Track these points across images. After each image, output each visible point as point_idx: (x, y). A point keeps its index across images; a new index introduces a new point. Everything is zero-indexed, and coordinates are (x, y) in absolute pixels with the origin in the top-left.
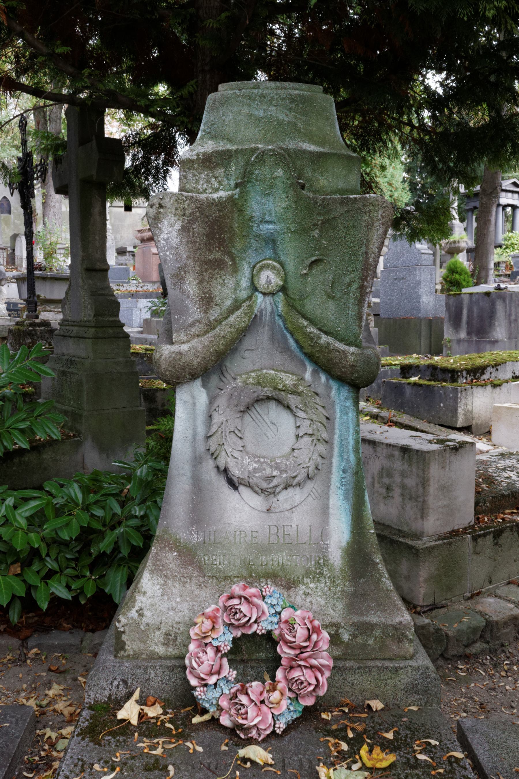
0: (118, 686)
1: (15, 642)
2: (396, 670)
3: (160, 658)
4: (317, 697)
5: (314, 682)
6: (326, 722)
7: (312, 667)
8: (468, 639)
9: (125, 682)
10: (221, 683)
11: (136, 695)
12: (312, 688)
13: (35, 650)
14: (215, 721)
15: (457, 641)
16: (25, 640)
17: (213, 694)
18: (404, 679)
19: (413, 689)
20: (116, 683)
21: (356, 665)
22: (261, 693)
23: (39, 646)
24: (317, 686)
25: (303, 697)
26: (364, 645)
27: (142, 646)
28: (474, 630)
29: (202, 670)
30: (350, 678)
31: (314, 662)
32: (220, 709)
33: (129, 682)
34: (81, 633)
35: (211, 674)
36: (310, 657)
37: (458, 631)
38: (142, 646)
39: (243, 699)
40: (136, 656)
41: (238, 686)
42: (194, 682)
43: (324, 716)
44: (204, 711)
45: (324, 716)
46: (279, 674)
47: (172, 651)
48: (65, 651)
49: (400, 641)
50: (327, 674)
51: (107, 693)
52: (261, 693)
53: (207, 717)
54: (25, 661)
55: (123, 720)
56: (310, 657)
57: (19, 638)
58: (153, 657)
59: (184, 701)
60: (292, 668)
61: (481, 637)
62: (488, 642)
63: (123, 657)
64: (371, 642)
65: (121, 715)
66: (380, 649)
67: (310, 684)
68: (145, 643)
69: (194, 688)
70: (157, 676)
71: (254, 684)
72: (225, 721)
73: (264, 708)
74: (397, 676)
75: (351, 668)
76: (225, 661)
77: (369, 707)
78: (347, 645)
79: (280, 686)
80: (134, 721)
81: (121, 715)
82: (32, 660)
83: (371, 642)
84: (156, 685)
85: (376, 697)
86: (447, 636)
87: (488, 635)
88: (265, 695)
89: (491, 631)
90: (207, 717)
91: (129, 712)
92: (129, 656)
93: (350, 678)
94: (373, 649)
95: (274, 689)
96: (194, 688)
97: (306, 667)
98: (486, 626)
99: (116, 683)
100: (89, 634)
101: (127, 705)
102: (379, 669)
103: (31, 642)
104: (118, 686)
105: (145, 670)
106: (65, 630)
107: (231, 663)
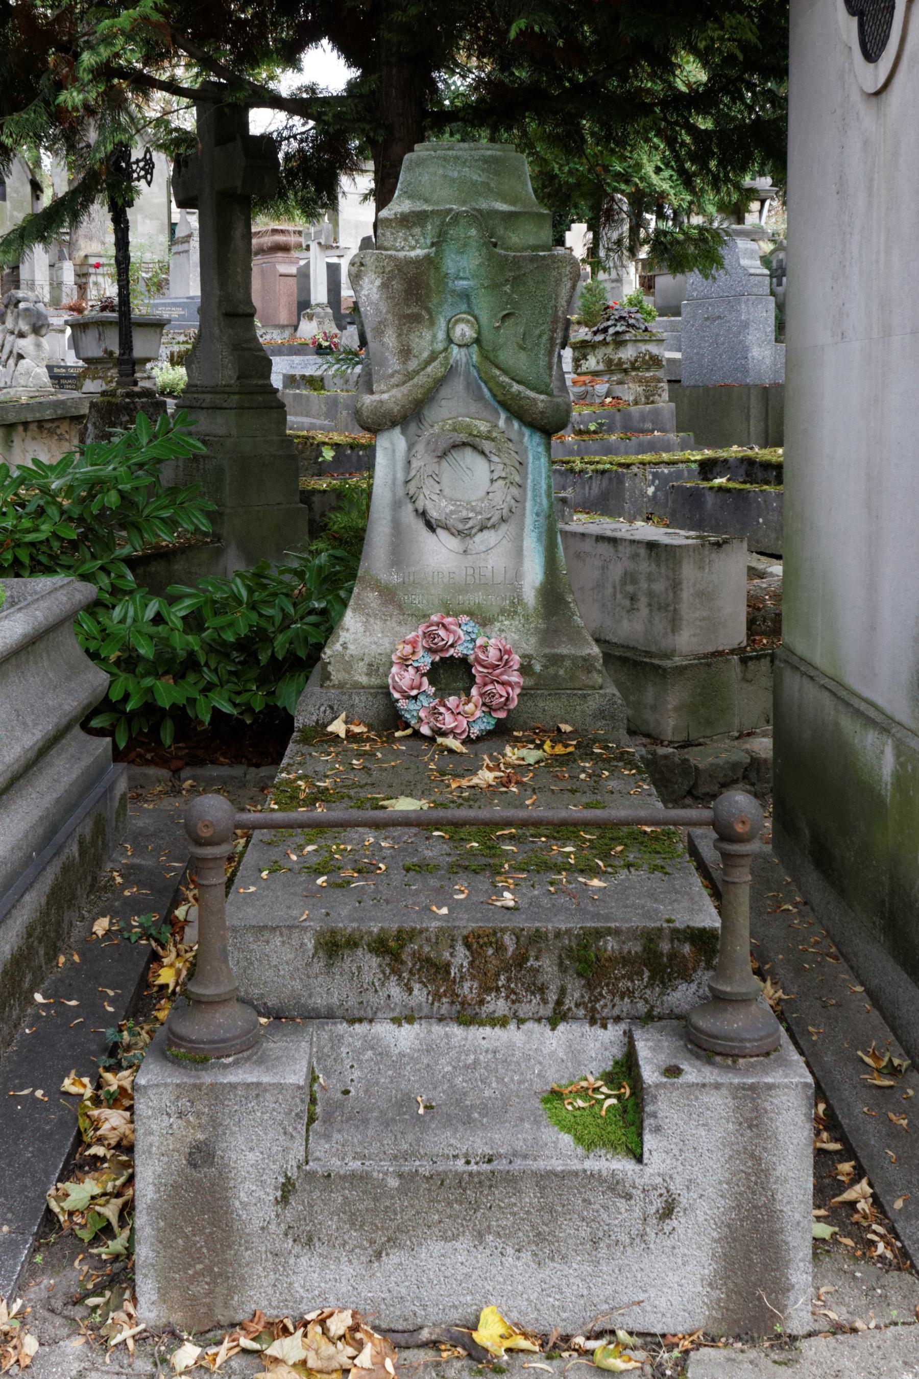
0: (325, 712)
1: (164, 773)
2: (585, 696)
3: (364, 687)
4: (509, 711)
5: (504, 694)
6: (517, 737)
7: (503, 684)
8: (725, 776)
9: (331, 707)
10: (421, 697)
11: (343, 716)
12: (503, 699)
13: (190, 782)
14: (417, 734)
15: (710, 776)
16: (176, 772)
17: (412, 706)
18: (593, 704)
19: (600, 714)
20: (323, 708)
21: (546, 693)
22: (458, 706)
23: (194, 778)
24: (507, 699)
25: (495, 710)
26: (556, 676)
27: (347, 676)
28: (735, 766)
29: (404, 684)
30: (541, 704)
31: (505, 678)
32: (420, 720)
33: (335, 707)
34: (244, 767)
35: (412, 688)
36: (502, 674)
37: (712, 764)
38: (347, 676)
39: (442, 710)
40: (341, 686)
41: (437, 701)
42: (396, 695)
43: (515, 733)
44: (407, 725)
45: (515, 733)
46: (474, 691)
47: (375, 681)
48: (225, 783)
49: (589, 672)
50: (518, 691)
51: (314, 718)
52: (458, 706)
53: (409, 731)
54: (180, 792)
55: (332, 733)
56: (502, 674)
57: (169, 769)
58: (357, 686)
60: (485, 685)
61: (745, 777)
62: (753, 784)
63: (328, 687)
64: (561, 672)
65: (330, 729)
66: (571, 678)
67: (501, 696)
68: (349, 673)
69: (397, 701)
70: (360, 701)
71: (451, 698)
72: (425, 730)
73: (460, 717)
74: (586, 702)
75: (542, 695)
76: (425, 680)
77: (559, 730)
78: (540, 676)
79: (474, 700)
80: (343, 735)
81: (330, 729)
82: (188, 791)
83: (561, 672)
84: (360, 711)
85: (566, 722)
86: (697, 768)
87: (753, 776)
88: (461, 707)
89: (758, 771)
90: (409, 731)
91: (338, 727)
92: (334, 686)
93: (541, 704)
94: (564, 679)
95: (469, 701)
96: (397, 701)
97: (498, 682)
98: (751, 764)
99: (323, 708)
100: (252, 769)
101: (335, 722)
102: (569, 696)
103: (184, 774)
104: (325, 712)
105: (350, 696)
106: (222, 764)
107: (431, 683)
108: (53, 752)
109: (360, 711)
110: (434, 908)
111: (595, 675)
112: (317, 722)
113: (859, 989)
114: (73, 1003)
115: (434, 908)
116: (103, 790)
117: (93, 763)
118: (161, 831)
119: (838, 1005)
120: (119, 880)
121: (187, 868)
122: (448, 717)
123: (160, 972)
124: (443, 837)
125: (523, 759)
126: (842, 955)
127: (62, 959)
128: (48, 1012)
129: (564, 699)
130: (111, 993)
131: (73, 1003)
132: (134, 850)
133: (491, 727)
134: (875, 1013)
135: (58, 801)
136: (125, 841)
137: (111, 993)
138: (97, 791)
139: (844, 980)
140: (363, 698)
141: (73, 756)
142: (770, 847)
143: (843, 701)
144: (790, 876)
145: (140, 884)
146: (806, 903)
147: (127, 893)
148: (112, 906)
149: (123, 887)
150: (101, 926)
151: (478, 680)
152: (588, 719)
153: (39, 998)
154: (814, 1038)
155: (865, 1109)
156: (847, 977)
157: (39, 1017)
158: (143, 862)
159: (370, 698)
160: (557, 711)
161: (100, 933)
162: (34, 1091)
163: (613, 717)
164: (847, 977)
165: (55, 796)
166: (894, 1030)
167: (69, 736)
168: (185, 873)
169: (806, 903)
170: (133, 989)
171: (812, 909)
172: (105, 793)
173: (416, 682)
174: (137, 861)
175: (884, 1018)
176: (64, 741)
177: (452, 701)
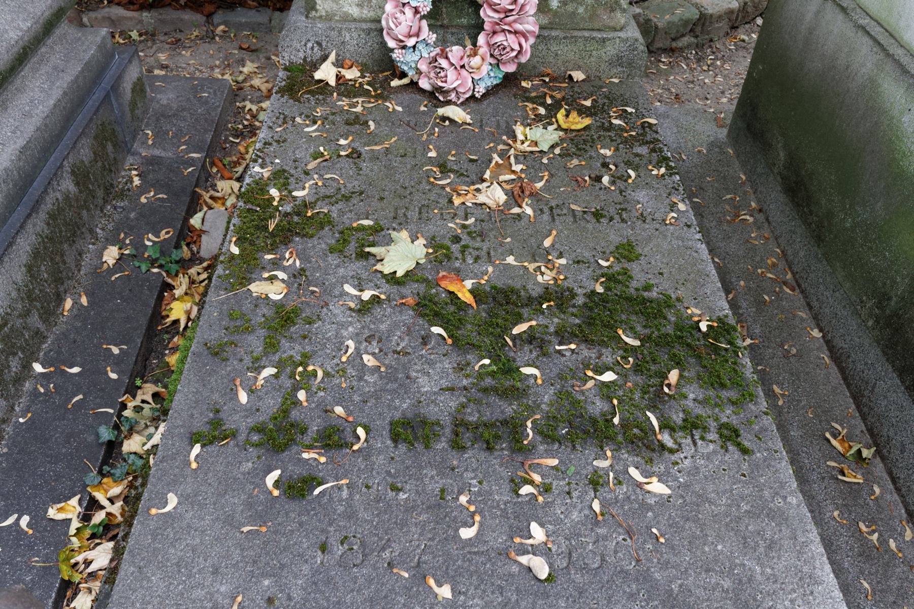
0: (312, 48)
1: (199, 18)
2: (604, 40)
3: (355, 20)
4: (519, 64)
5: (517, 47)
6: (526, 90)
7: (516, 33)
8: (678, 32)
9: (319, 44)
10: (420, 46)
11: (332, 57)
12: (514, 54)
13: (222, 27)
14: (414, 84)
15: (666, 33)
16: (209, 16)
17: (411, 57)
18: (611, 50)
19: (618, 61)
20: (310, 45)
21: (562, 35)
22: (462, 58)
23: (225, 23)
24: (520, 52)
25: (504, 63)
26: (574, 13)
27: (335, 7)
28: (686, 22)
29: (400, 31)
30: (554, 48)
31: (518, 27)
32: (419, 72)
33: (324, 44)
34: (269, 11)
35: (409, 36)
36: (515, 21)
37: (669, 23)
38: (335, 7)
39: (444, 63)
40: (329, 18)
41: (438, 50)
42: (391, 44)
43: (524, 84)
44: (403, 75)
45: (524, 84)
46: (481, 39)
47: (367, 13)
48: (254, 30)
49: (613, 10)
50: (532, 40)
51: (301, 55)
52: (462, 58)
53: (405, 81)
54: (213, 38)
55: (321, 81)
56: (515, 21)
57: (202, 13)
58: (347, 19)
59: (383, 65)
60: (494, 33)
61: (691, 31)
62: (697, 37)
63: (314, 18)
64: (581, 10)
65: (318, 75)
66: (591, 18)
67: (512, 50)
68: (337, 4)
69: (392, 50)
70: (352, 39)
71: (455, 48)
72: (424, 84)
73: (464, 72)
74: (604, 47)
75: (556, 38)
76: (424, 23)
77: (570, 77)
78: (556, 13)
79: (481, 51)
80: (332, 82)
81: (318, 75)
82: (221, 37)
83: (581, 10)
84: (352, 49)
85: (579, 68)
86: (656, 27)
87: (698, 30)
88: (466, 60)
89: (703, 24)
90: (405, 81)
91: (327, 73)
92: (321, 17)
93: (554, 48)
94: (583, 18)
95: (475, 54)
96: (392, 50)
97: (510, 32)
98: (699, 20)
99: (310, 45)
100: (277, 13)
101: (324, 66)
102: (586, 39)
103: (217, 18)
104: (312, 48)
105: (340, 32)
106: (250, 8)
107: (431, 27)
108: (26, 71)
109: (352, 49)
110: (432, 582)
111: (619, 15)
112: (305, 59)
113: (816, 333)
114: (76, 370)
115: (432, 582)
116: (103, 94)
117: (82, 72)
118: (184, 110)
119: (799, 355)
120: (137, 181)
121: (206, 158)
122: (451, 74)
123: (172, 306)
124: (444, 339)
125: (536, 144)
126: (798, 285)
127: (68, 303)
128: (46, 387)
129: (580, 44)
130: (116, 350)
131: (76, 370)
132: (156, 135)
133: (498, 81)
134: (834, 370)
135: (24, 150)
136: (147, 125)
137: (116, 350)
138: (98, 96)
139: (802, 319)
140: (355, 35)
141: (55, 68)
142: (725, 131)
143: (897, 62)
144: (745, 174)
145: (157, 186)
146: (760, 211)
147: (143, 200)
148: (128, 218)
149: (142, 190)
150: (111, 255)
151: (487, 26)
152: (603, 66)
153: (38, 368)
154: (780, 403)
155: (836, 513)
156: (804, 315)
157: (35, 394)
158: (163, 154)
159: (363, 36)
160: (571, 56)
161: (111, 262)
162: (18, 519)
163: (630, 64)
164: (804, 315)
165: (21, 142)
166: (857, 397)
167: (49, 42)
168: (205, 161)
169: (760, 211)
170: (139, 341)
171: (767, 219)
172: (107, 96)
173: (414, 30)
174: (157, 152)
175: (845, 379)
176: (43, 50)
177: (455, 51)
